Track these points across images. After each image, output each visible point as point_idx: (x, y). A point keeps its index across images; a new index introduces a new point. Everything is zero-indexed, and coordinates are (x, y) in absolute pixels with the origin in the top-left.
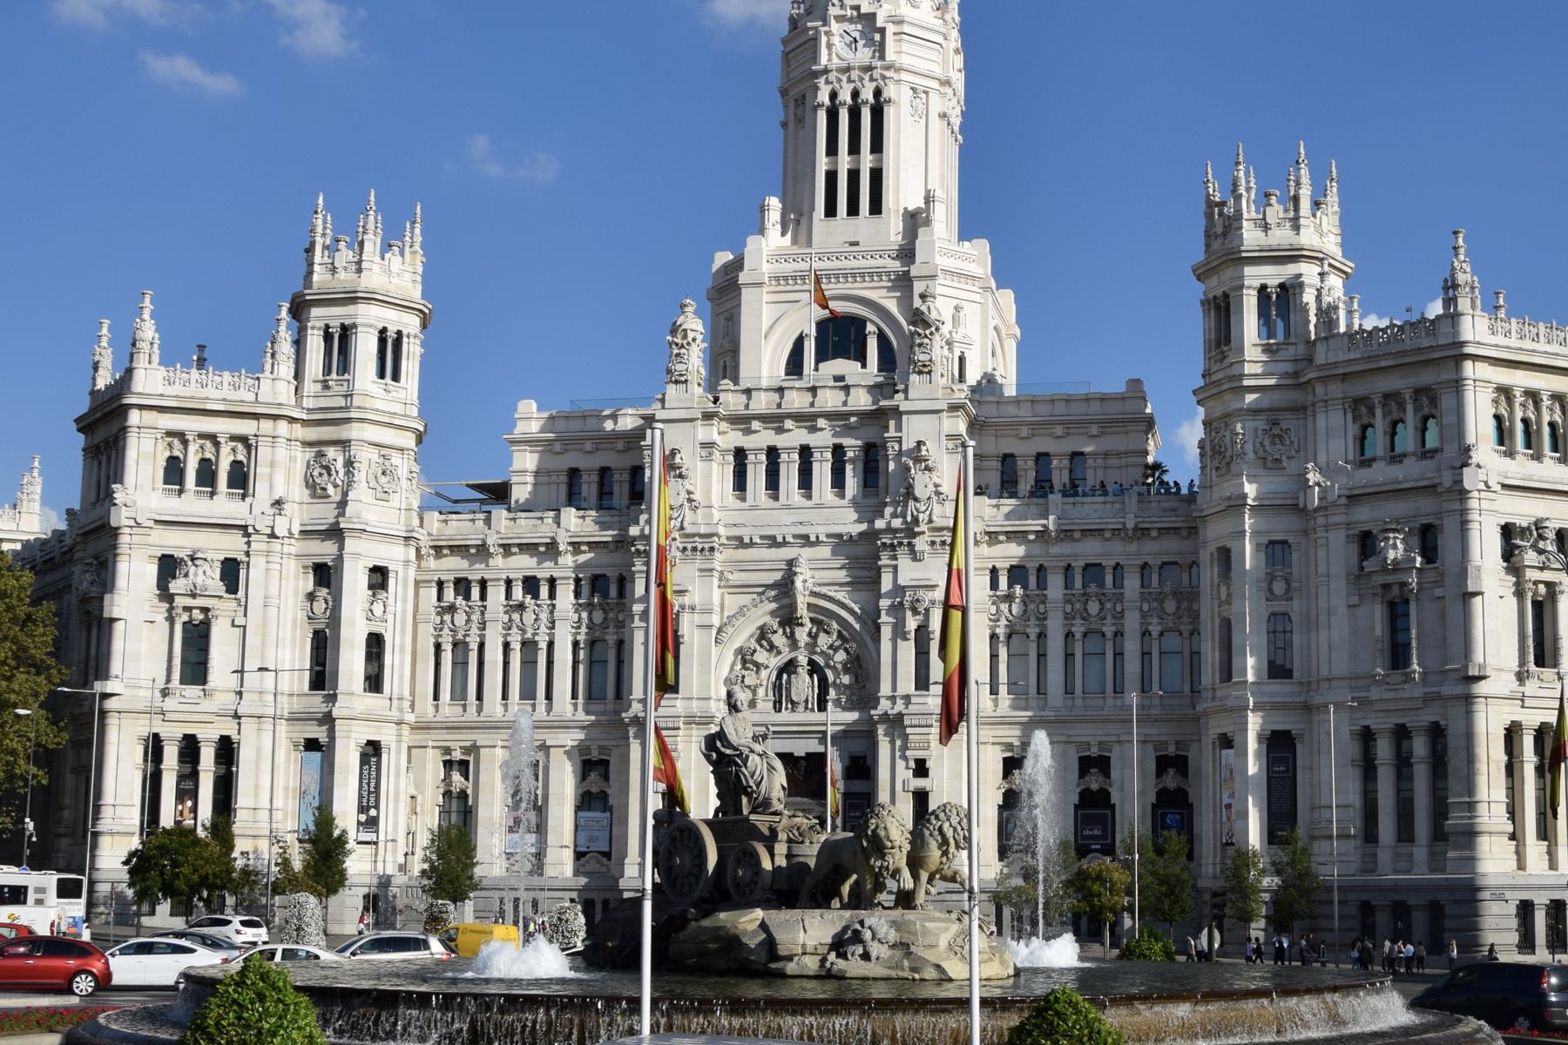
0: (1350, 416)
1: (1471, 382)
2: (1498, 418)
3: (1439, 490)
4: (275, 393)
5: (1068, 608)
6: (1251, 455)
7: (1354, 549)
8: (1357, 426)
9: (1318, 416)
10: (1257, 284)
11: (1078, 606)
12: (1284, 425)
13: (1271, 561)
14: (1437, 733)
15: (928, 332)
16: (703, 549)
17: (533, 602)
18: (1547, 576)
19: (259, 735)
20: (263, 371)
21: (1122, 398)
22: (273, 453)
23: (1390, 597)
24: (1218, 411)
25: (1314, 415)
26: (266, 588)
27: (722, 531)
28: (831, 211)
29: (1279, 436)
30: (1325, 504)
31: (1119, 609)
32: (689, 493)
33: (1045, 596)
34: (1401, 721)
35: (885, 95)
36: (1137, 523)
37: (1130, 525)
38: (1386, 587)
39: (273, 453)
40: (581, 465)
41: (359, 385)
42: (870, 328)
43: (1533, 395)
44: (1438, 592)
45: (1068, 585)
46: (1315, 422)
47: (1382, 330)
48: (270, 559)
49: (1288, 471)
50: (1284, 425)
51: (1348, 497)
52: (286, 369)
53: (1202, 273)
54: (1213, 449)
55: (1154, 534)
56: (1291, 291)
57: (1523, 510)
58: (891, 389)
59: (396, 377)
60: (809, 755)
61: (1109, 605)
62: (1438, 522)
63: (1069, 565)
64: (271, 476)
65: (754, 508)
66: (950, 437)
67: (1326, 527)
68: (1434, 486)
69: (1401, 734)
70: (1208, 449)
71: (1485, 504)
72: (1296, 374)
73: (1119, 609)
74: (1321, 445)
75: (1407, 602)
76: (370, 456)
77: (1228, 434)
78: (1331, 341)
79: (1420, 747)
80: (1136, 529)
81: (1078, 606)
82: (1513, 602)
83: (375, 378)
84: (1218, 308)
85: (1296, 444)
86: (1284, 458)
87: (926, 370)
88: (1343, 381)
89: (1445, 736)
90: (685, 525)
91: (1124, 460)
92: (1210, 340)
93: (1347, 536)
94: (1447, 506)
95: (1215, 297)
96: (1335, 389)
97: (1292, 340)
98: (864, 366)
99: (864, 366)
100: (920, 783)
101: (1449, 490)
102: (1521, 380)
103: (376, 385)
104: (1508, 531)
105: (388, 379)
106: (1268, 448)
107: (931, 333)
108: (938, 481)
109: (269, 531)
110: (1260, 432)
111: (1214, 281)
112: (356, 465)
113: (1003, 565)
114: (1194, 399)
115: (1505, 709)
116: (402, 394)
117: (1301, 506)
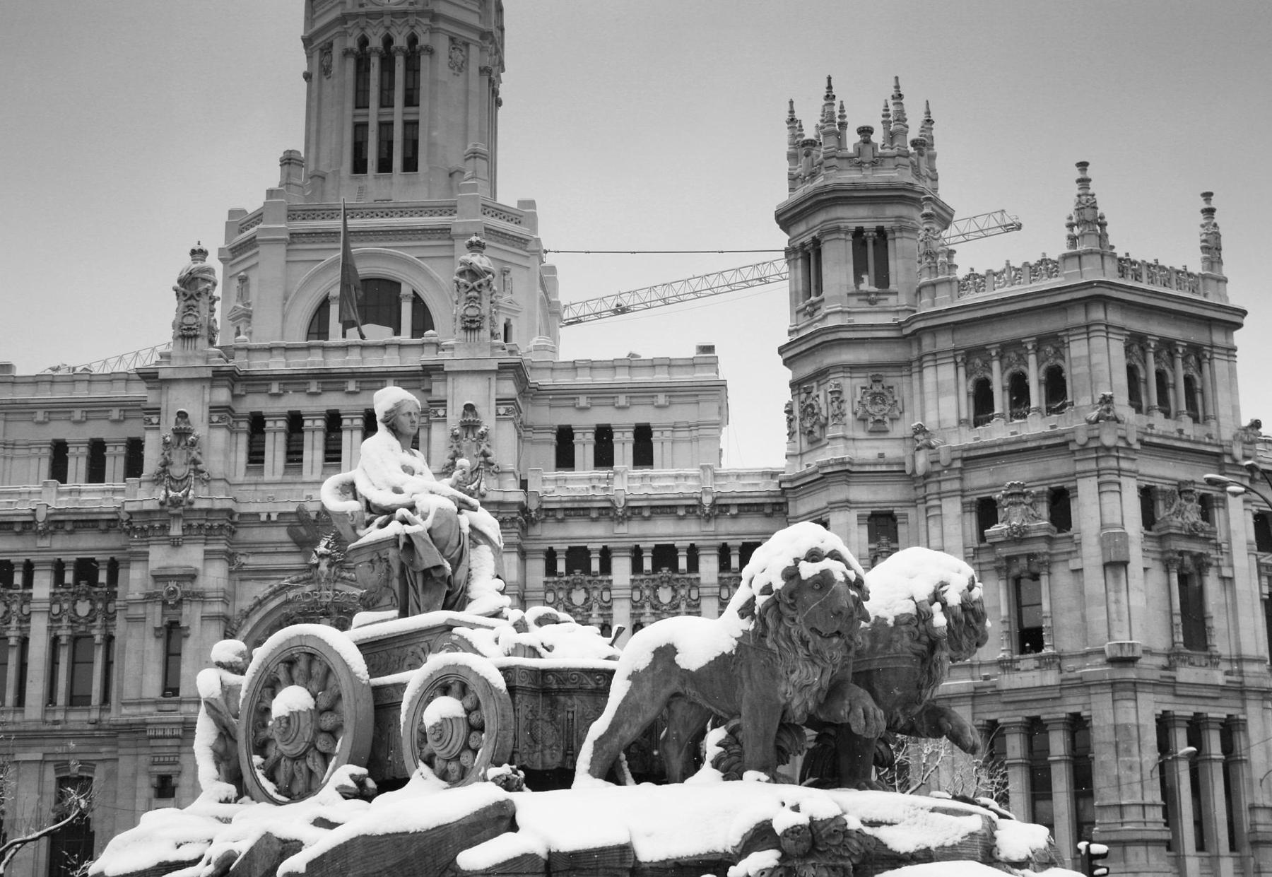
0: (962, 371)
1: (1103, 328)
2: (1132, 371)
3: (1072, 447)
5: (637, 596)
6: (849, 416)
7: (972, 521)
8: (971, 382)
9: (926, 371)
10: (853, 226)
11: (647, 592)
12: (889, 381)
13: (873, 537)
14: (1077, 725)
15: (475, 284)
16: (211, 527)
18: (1197, 548)
21: (692, 364)
23: (1015, 571)
24: (808, 369)
25: (921, 372)
28: (359, 166)
29: (881, 394)
30: (937, 468)
31: (694, 595)
33: (610, 581)
34: (1034, 713)
35: (424, 40)
36: (715, 500)
37: (707, 500)
38: (1009, 559)
40: (68, 438)
42: (405, 290)
43: (1167, 345)
44: (1074, 564)
45: (637, 567)
46: (921, 378)
47: (995, 274)
49: (890, 435)
50: (889, 381)
51: (964, 460)
53: (787, 219)
54: (804, 411)
55: (734, 511)
56: (890, 236)
57: (1165, 472)
61: (683, 592)
62: (1071, 485)
63: (637, 547)
66: (500, 401)
67: (941, 495)
68: (1066, 444)
69: (1034, 728)
70: (797, 413)
71: (1124, 465)
72: (899, 326)
73: (694, 595)
74: (930, 404)
75: (1036, 577)
77: (822, 394)
78: (940, 289)
79: (1058, 744)
80: (714, 505)
81: (647, 592)
82: (1157, 575)
84: (807, 258)
85: (900, 405)
86: (886, 419)
87: (474, 326)
88: (953, 331)
89: (1088, 729)
91: (695, 433)
92: (797, 292)
93: (963, 504)
94: (1080, 467)
95: (803, 245)
96: (945, 342)
97: (892, 287)
98: (397, 332)
99: (397, 332)
101: (1084, 448)
102: (1157, 329)
104: (1148, 496)
106: (868, 408)
107: (480, 286)
108: (488, 450)
110: (858, 390)
111: (802, 228)
113: (560, 547)
114: (780, 359)
115: (1159, 698)
117: (908, 472)
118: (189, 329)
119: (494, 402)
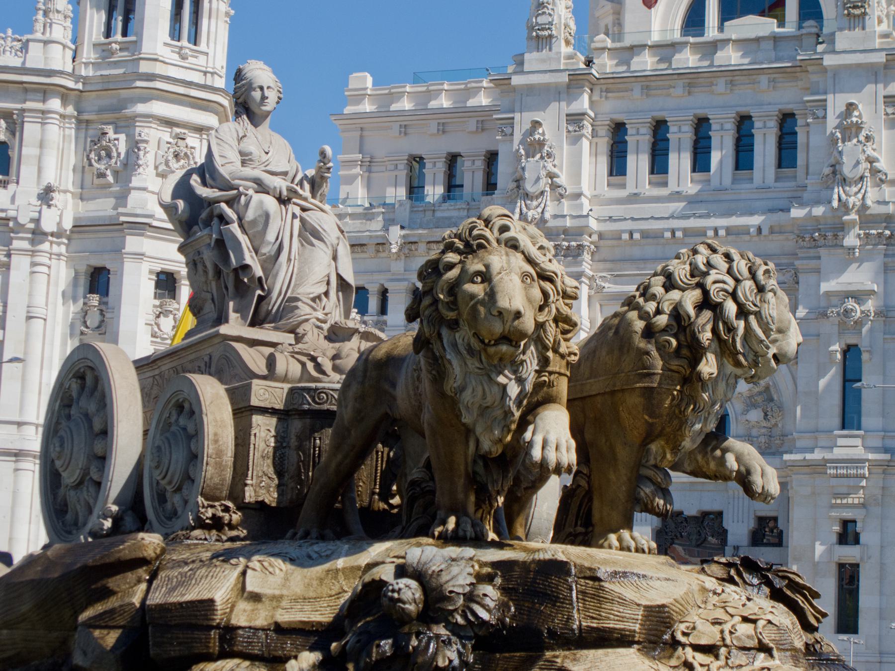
4: (46, 58)
17: (358, 317)
19: (16, 476)
20: (32, 31)
22: (43, 131)
26: (30, 295)
27: (593, 224)
32: (551, 176)
39: (43, 131)
41: (147, 48)
48: (38, 259)
52: (61, 31)
58: (814, 40)
59: (195, 39)
60: (705, 514)
64: (40, 159)
65: (634, 198)
76: (159, 134)
83: (169, 40)
87: (857, 12)
90: (547, 216)
100: (849, 554)
103: (169, 49)
105: (184, 42)
109: (32, 226)
112: (142, 146)
116: (201, 61)
118: (543, 29)
119: (881, 100)
